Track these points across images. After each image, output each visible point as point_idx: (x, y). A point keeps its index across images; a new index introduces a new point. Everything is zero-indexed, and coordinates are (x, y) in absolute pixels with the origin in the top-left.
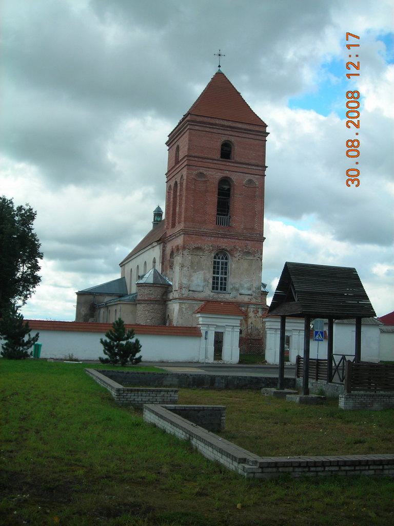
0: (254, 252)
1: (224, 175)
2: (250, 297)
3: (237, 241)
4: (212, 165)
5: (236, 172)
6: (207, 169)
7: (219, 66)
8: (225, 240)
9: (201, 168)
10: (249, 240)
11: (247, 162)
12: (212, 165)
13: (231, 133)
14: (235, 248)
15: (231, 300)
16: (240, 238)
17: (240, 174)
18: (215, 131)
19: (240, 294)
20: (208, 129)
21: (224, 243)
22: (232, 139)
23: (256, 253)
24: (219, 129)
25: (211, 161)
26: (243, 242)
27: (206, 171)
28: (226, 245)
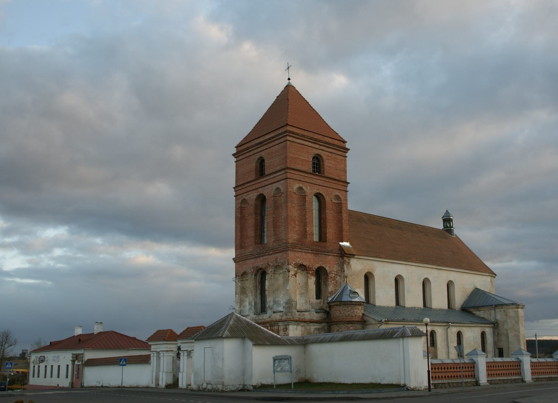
0: (282, 263)
1: (258, 193)
2: (281, 314)
3: (269, 256)
4: (250, 188)
5: (267, 185)
6: (248, 193)
7: (289, 79)
8: (261, 258)
9: (244, 195)
10: (277, 253)
11: (275, 171)
12: (250, 188)
13: (262, 148)
14: (268, 264)
15: (268, 320)
16: (270, 253)
17: (269, 186)
18: (251, 153)
19: (274, 312)
20: (247, 155)
21: (260, 262)
22: (263, 154)
23: (284, 265)
24: (253, 150)
25: (248, 185)
26: (274, 256)
27: (247, 195)
28: (262, 264)
